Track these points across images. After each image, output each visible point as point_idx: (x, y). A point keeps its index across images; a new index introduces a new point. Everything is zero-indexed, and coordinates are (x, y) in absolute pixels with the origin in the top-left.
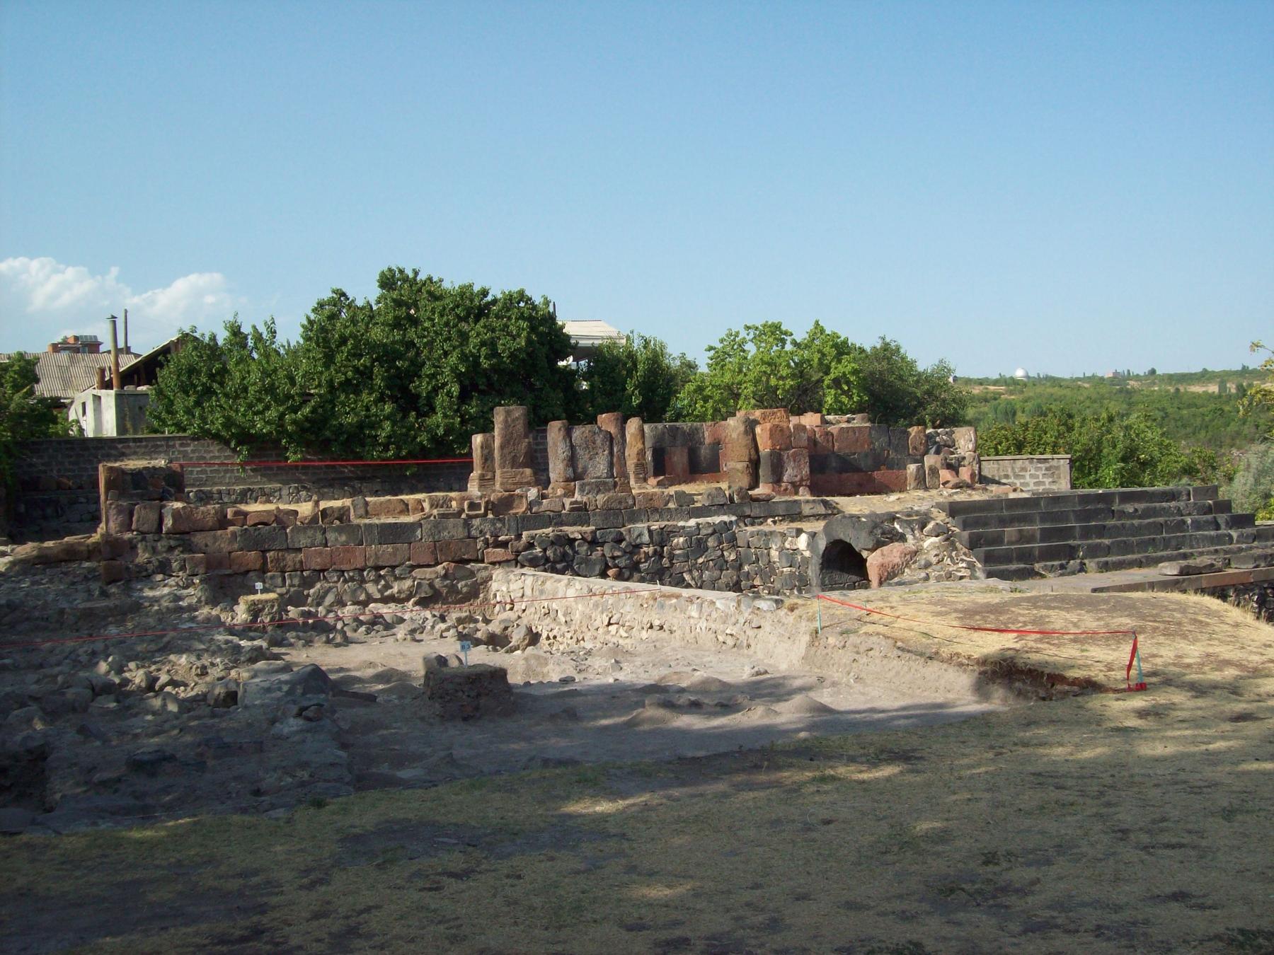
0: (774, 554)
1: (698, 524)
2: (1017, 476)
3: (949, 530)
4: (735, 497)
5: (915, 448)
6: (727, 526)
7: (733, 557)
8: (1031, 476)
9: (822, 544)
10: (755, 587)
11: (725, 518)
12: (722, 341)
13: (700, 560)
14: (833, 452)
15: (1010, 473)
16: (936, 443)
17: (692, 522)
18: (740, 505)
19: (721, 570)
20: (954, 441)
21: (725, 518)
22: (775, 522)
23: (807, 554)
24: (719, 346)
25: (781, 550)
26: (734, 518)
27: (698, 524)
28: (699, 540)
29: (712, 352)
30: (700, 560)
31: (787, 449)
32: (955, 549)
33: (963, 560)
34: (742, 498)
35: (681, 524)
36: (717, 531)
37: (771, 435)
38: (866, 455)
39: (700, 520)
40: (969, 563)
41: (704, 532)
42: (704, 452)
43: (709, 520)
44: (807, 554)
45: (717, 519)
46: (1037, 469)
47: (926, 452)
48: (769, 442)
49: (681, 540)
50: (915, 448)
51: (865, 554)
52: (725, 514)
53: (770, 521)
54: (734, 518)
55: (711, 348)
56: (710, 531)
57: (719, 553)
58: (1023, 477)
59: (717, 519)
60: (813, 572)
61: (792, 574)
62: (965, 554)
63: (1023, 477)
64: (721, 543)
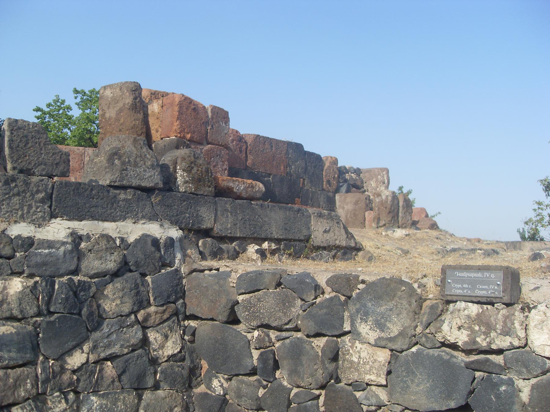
1: (77, 238)
4: (181, 176)
5: (329, 182)
6: (156, 253)
7: (171, 348)
11: (154, 229)
12: (49, 105)
13: (76, 359)
14: (246, 168)
16: (346, 181)
17: (58, 230)
18: (192, 198)
19: (139, 390)
20: (362, 182)
21: (154, 229)
22: (262, 254)
24: (46, 109)
26: (175, 233)
28: (76, 291)
29: (39, 113)
30: (76, 359)
31: (200, 143)
34: (198, 181)
35: (20, 229)
36: (136, 262)
37: (180, 113)
39: (84, 227)
41: (93, 264)
43: (110, 228)
45: (133, 230)
47: (337, 191)
48: (176, 125)
49: (16, 285)
50: (329, 182)
53: (252, 249)
54: (175, 233)
55: (38, 109)
57: (134, 335)
59: (133, 230)
64: (141, 303)
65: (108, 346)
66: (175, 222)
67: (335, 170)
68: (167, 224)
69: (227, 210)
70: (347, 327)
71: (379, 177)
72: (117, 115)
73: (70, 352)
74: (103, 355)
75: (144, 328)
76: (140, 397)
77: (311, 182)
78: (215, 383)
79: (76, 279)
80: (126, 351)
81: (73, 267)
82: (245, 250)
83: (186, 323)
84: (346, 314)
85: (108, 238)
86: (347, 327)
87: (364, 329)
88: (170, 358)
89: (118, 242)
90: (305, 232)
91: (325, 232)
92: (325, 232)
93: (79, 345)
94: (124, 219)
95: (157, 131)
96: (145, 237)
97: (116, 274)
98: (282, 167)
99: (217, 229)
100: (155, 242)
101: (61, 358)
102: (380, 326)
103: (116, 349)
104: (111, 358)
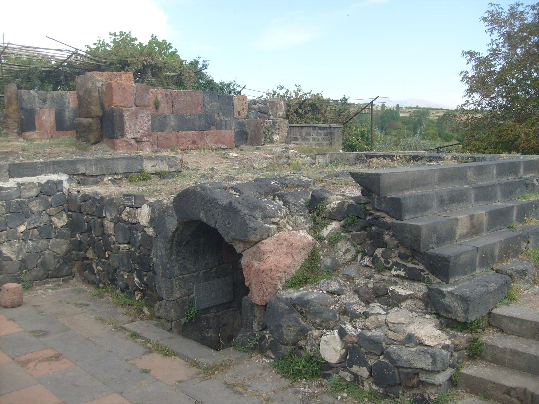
0: (109, 225)
2: (303, 139)
3: (366, 213)
8: (314, 139)
9: (172, 224)
10: (88, 259)
11: (54, 177)
13: (22, 228)
15: (298, 137)
17: (12, 183)
21: (54, 177)
23: (150, 231)
25: (117, 221)
27: (18, 184)
28: (20, 204)
30: (22, 228)
32: (384, 245)
33: (399, 266)
38: (200, 116)
40: (409, 270)
42: (68, 115)
43: (34, 179)
44: (150, 231)
45: (43, 179)
46: (318, 134)
51: (239, 248)
52: (54, 173)
54: (64, 177)
56: (34, 193)
57: (45, 218)
58: (308, 139)
59: (43, 179)
60: (158, 255)
61: (130, 255)
62: (402, 257)
63: (308, 139)
65: (36, 222)
66: (65, 172)
67: (244, 104)
68: (61, 174)
69: (92, 164)
70: (104, 215)
73: (19, 226)
74: (33, 227)
75: (50, 216)
76: (49, 242)
77: (224, 114)
78: (77, 236)
79: (19, 200)
80: (42, 225)
81: (18, 196)
82: (103, 180)
83: (69, 213)
84: (104, 210)
85: (33, 183)
86: (104, 215)
87: (108, 215)
88: (62, 227)
89: (37, 184)
90: (140, 168)
91: (153, 166)
92: (153, 166)
93: (22, 223)
94: (41, 175)
96: (48, 181)
97: (37, 196)
98: (200, 108)
99: (88, 173)
100: (53, 182)
101: (15, 228)
102: (111, 215)
103: (38, 224)
104: (36, 228)
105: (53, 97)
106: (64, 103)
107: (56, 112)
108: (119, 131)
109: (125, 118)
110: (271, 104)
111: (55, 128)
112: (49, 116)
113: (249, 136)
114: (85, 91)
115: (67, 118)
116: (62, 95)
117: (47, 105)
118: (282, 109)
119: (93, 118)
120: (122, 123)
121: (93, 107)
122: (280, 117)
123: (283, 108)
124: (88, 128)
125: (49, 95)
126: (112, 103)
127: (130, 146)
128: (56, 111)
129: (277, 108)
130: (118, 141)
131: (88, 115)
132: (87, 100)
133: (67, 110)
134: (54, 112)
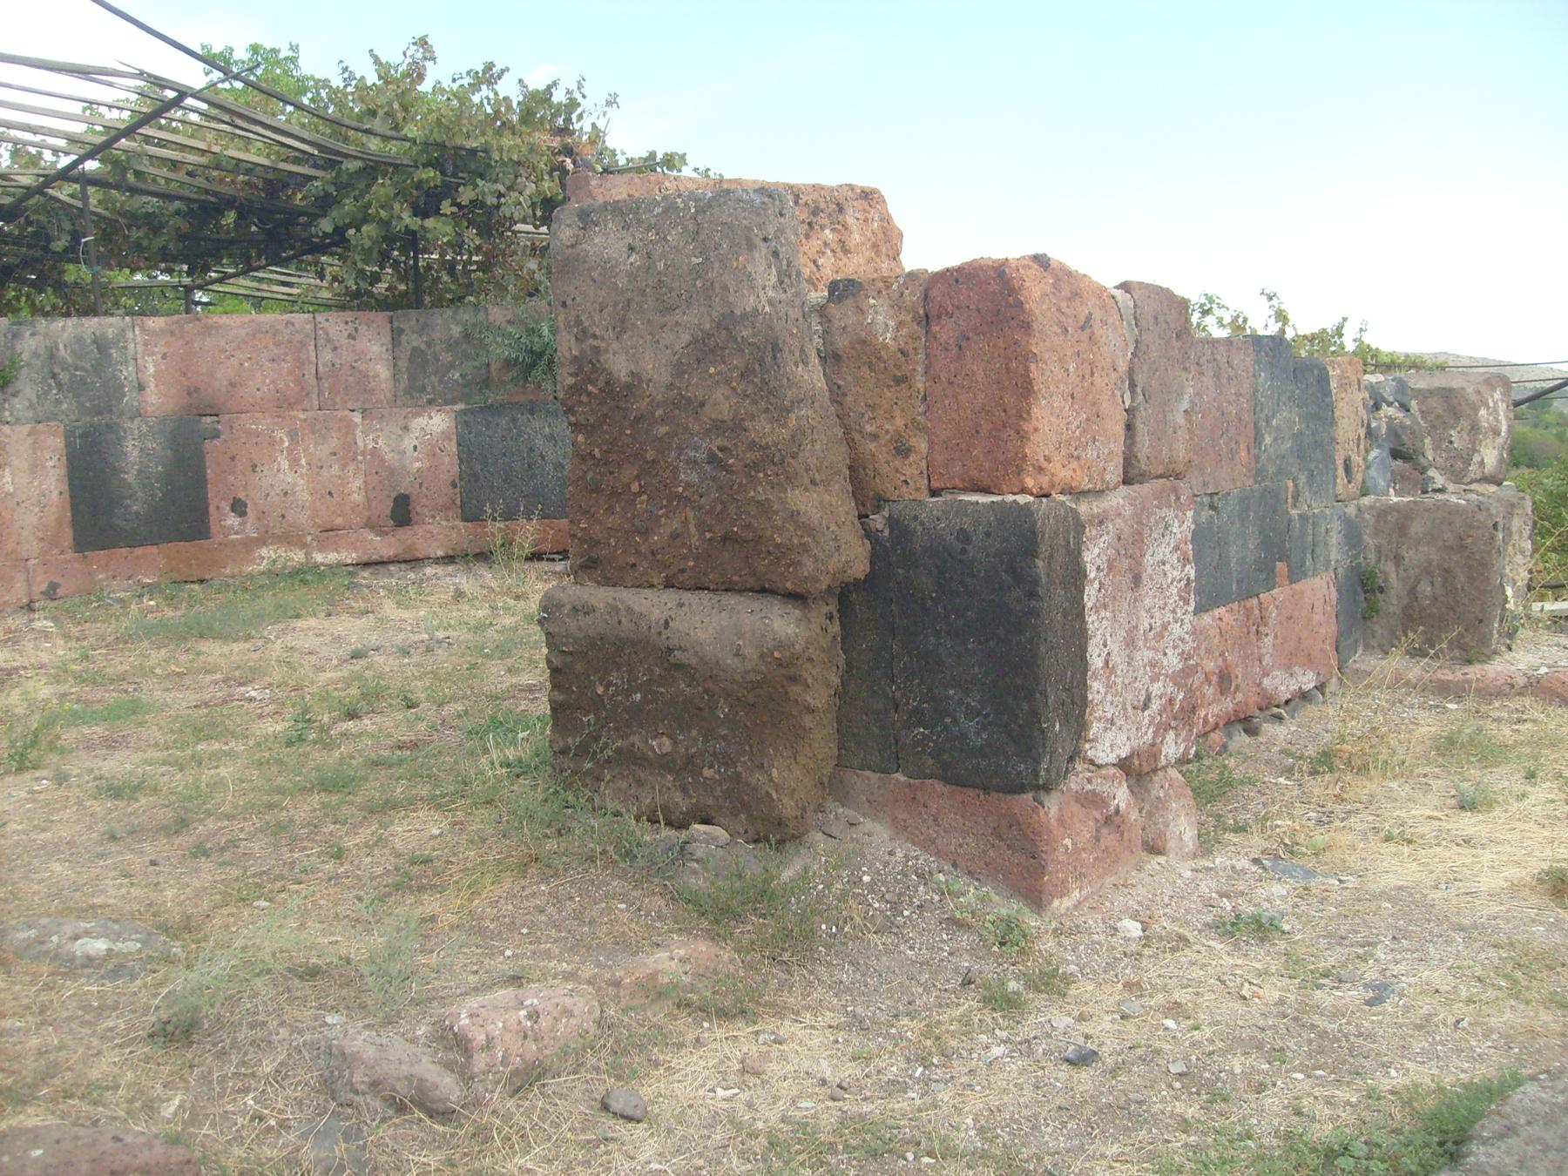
42: (137, 454)
71: (1483, 412)
72: (679, 370)
95: (903, 451)
105: (52, 354)
106: (114, 390)
107: (68, 445)
108: (1065, 722)
109: (1091, 595)
110: (1435, 404)
111: (68, 533)
112: (35, 468)
113: (1393, 603)
114: (706, 348)
115: (130, 477)
116: (101, 344)
117: (19, 404)
118: (1497, 433)
119: (797, 598)
120: (1080, 638)
121: (806, 502)
122: (1485, 479)
123: (1504, 428)
124: (764, 700)
125: (29, 345)
126: (1017, 464)
127: (1109, 839)
128: (69, 434)
129: (1475, 428)
130: (1053, 806)
131: (743, 560)
132: (736, 427)
133: (134, 426)
134: (58, 442)
